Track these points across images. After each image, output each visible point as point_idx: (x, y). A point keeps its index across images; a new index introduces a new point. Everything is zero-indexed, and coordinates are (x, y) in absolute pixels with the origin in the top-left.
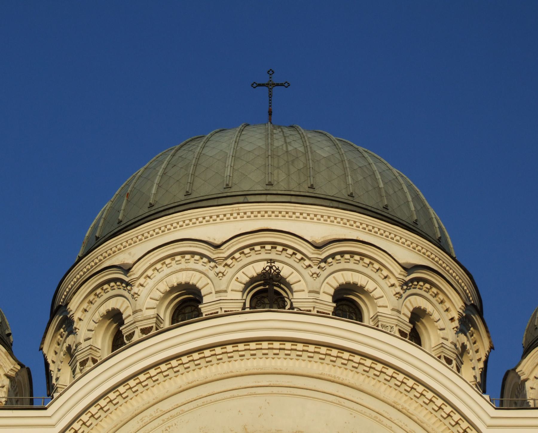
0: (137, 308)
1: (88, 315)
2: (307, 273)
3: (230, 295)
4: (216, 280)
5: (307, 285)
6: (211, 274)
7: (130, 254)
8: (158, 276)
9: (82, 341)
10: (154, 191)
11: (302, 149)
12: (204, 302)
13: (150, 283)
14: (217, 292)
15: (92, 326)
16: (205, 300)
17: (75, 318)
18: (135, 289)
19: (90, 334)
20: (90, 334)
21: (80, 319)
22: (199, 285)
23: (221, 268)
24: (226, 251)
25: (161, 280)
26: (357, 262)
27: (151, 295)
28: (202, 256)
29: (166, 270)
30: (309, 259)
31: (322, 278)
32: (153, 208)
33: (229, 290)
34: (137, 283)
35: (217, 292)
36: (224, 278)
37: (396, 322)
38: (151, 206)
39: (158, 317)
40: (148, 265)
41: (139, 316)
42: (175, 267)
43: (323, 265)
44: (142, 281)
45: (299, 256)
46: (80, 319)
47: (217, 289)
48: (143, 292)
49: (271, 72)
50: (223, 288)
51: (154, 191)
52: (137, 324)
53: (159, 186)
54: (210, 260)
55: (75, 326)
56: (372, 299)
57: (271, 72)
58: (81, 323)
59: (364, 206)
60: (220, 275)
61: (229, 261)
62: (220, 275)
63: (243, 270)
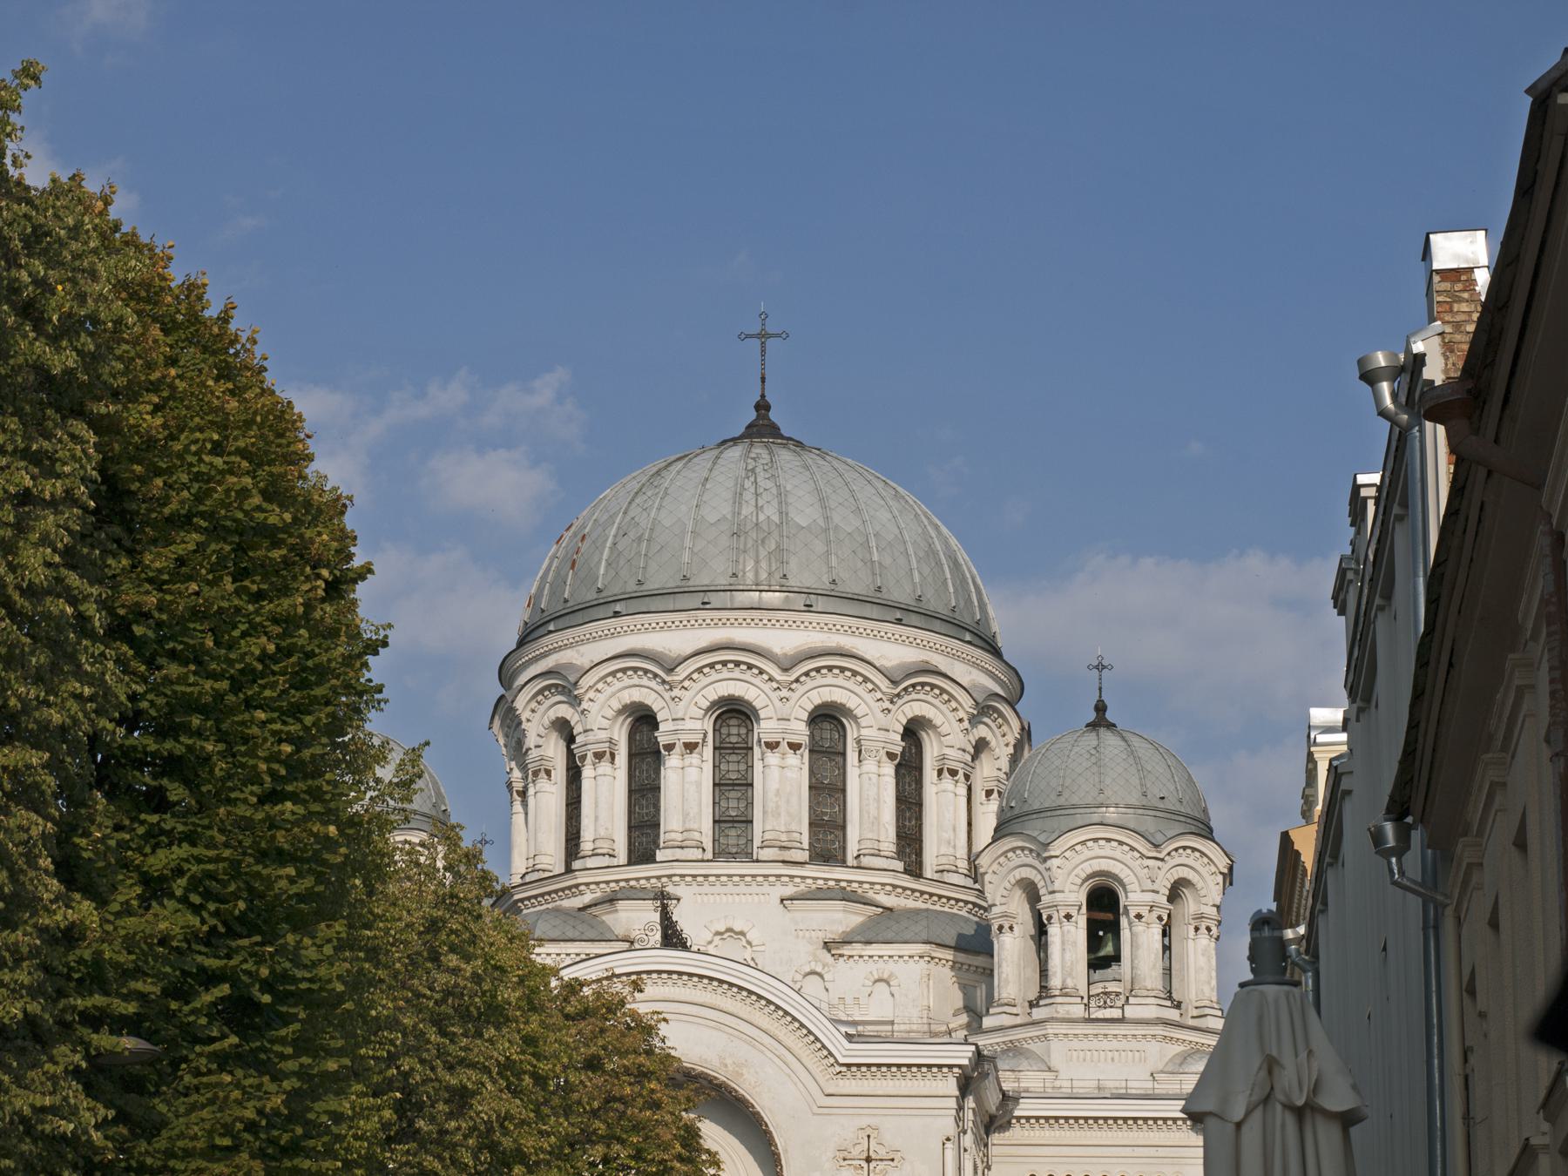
0: (588, 727)
1: (537, 715)
2: (775, 696)
3: (689, 724)
4: (672, 704)
5: (776, 712)
6: (667, 695)
7: (578, 652)
8: (609, 690)
9: (532, 747)
10: (602, 571)
12: (661, 730)
13: (601, 698)
14: (673, 720)
15: (542, 731)
16: (662, 727)
17: (523, 718)
18: (585, 705)
19: (541, 741)
20: (541, 741)
21: (528, 720)
22: (655, 708)
23: (676, 692)
24: (682, 672)
25: (614, 694)
26: (836, 676)
27: (602, 713)
28: (656, 676)
29: (618, 685)
30: (778, 682)
31: (792, 702)
32: (603, 595)
33: (687, 718)
34: (586, 698)
35: (673, 720)
36: (681, 703)
37: (883, 745)
38: (599, 591)
39: (611, 741)
40: (597, 678)
41: (591, 737)
42: (627, 682)
43: (794, 686)
44: (591, 694)
45: (765, 677)
46: (528, 720)
47: (674, 717)
48: (593, 708)
50: (680, 715)
51: (602, 571)
52: (589, 747)
53: (609, 564)
54: (664, 682)
55: (523, 727)
56: (855, 718)
58: (529, 724)
59: (850, 596)
60: (677, 700)
61: (686, 684)
62: (677, 700)
63: (703, 692)
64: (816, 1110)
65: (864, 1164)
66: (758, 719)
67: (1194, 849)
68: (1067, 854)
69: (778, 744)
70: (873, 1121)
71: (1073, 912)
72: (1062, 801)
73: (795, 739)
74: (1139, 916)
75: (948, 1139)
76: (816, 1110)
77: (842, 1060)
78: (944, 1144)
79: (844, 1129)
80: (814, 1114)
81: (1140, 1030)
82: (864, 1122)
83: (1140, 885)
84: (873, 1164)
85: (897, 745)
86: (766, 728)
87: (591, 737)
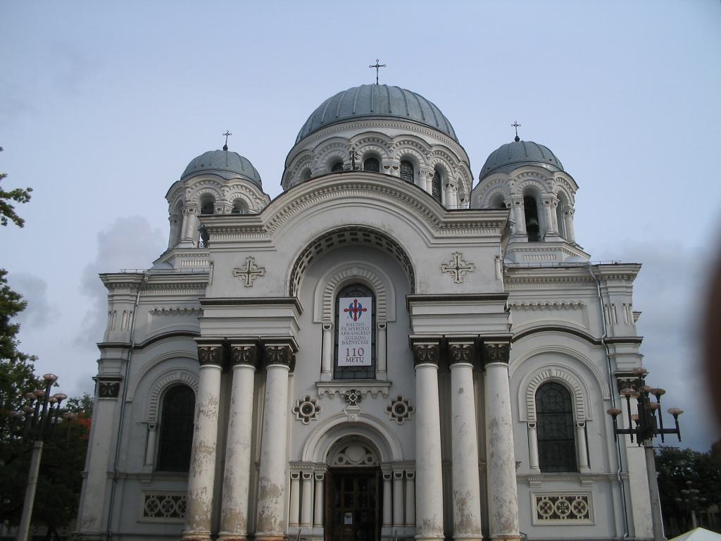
11: (386, 95)
18: (316, 159)
41: (318, 171)
48: (319, 161)
49: (378, 61)
57: (378, 61)
64: (430, 245)
65: (455, 271)
66: (381, 159)
67: (565, 181)
68: (516, 179)
69: (389, 167)
70: (459, 250)
72: (511, 161)
73: (396, 165)
74: (547, 202)
75: (497, 257)
76: (430, 245)
77: (443, 220)
78: (495, 260)
79: (443, 255)
80: (430, 247)
81: (553, 246)
82: (454, 250)
83: (547, 190)
84: (460, 271)
85: (433, 172)
86: (385, 161)
87: (318, 171)
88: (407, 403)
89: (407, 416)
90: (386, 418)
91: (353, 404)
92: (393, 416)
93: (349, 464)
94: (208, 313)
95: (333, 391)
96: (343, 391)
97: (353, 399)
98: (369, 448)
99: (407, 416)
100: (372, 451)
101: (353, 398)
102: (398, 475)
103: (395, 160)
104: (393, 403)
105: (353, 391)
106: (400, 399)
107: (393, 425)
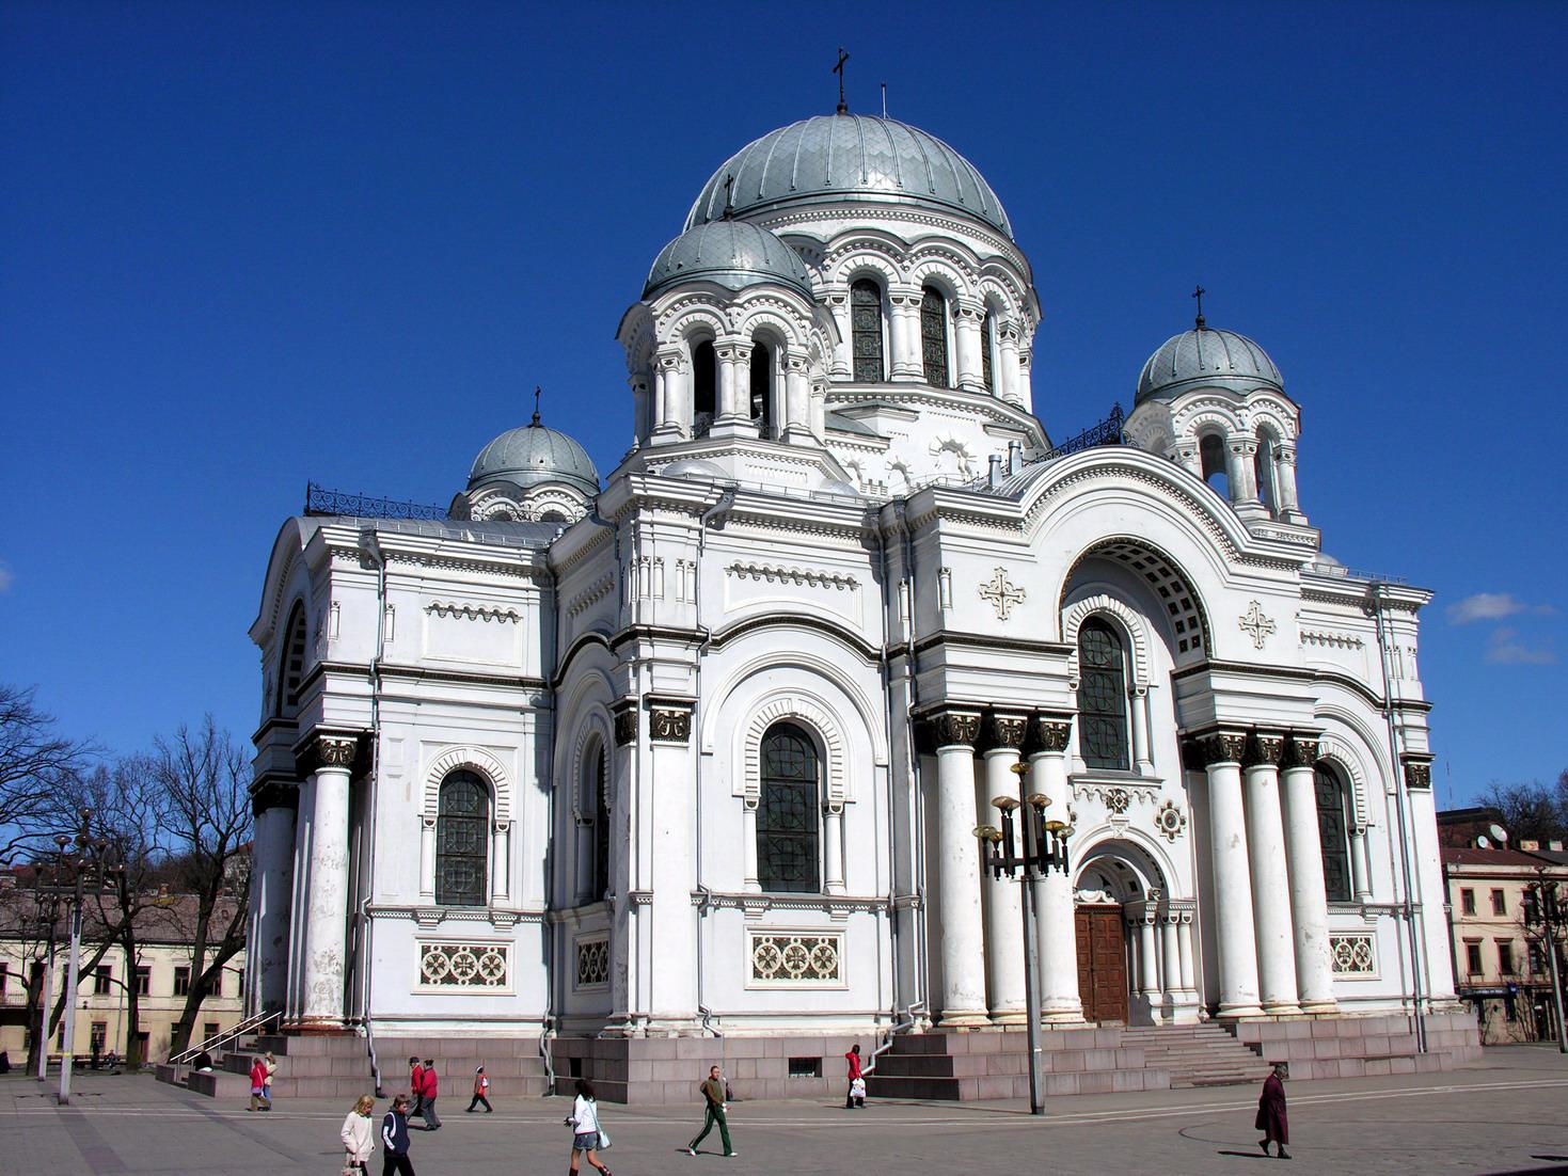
71: (1190, 450)
88: (1163, 811)
89: (1179, 831)
90: (1155, 833)
91: (1120, 811)
92: (1164, 831)
93: (1083, 901)
94: (954, 655)
95: (1091, 788)
96: (1105, 789)
97: (1116, 803)
98: (1108, 878)
99: (1179, 831)
100: (1110, 882)
101: (1119, 801)
102: (1174, 919)
103: (912, 286)
104: (1163, 811)
105: (1118, 791)
106: (1169, 805)
107: (1163, 841)
